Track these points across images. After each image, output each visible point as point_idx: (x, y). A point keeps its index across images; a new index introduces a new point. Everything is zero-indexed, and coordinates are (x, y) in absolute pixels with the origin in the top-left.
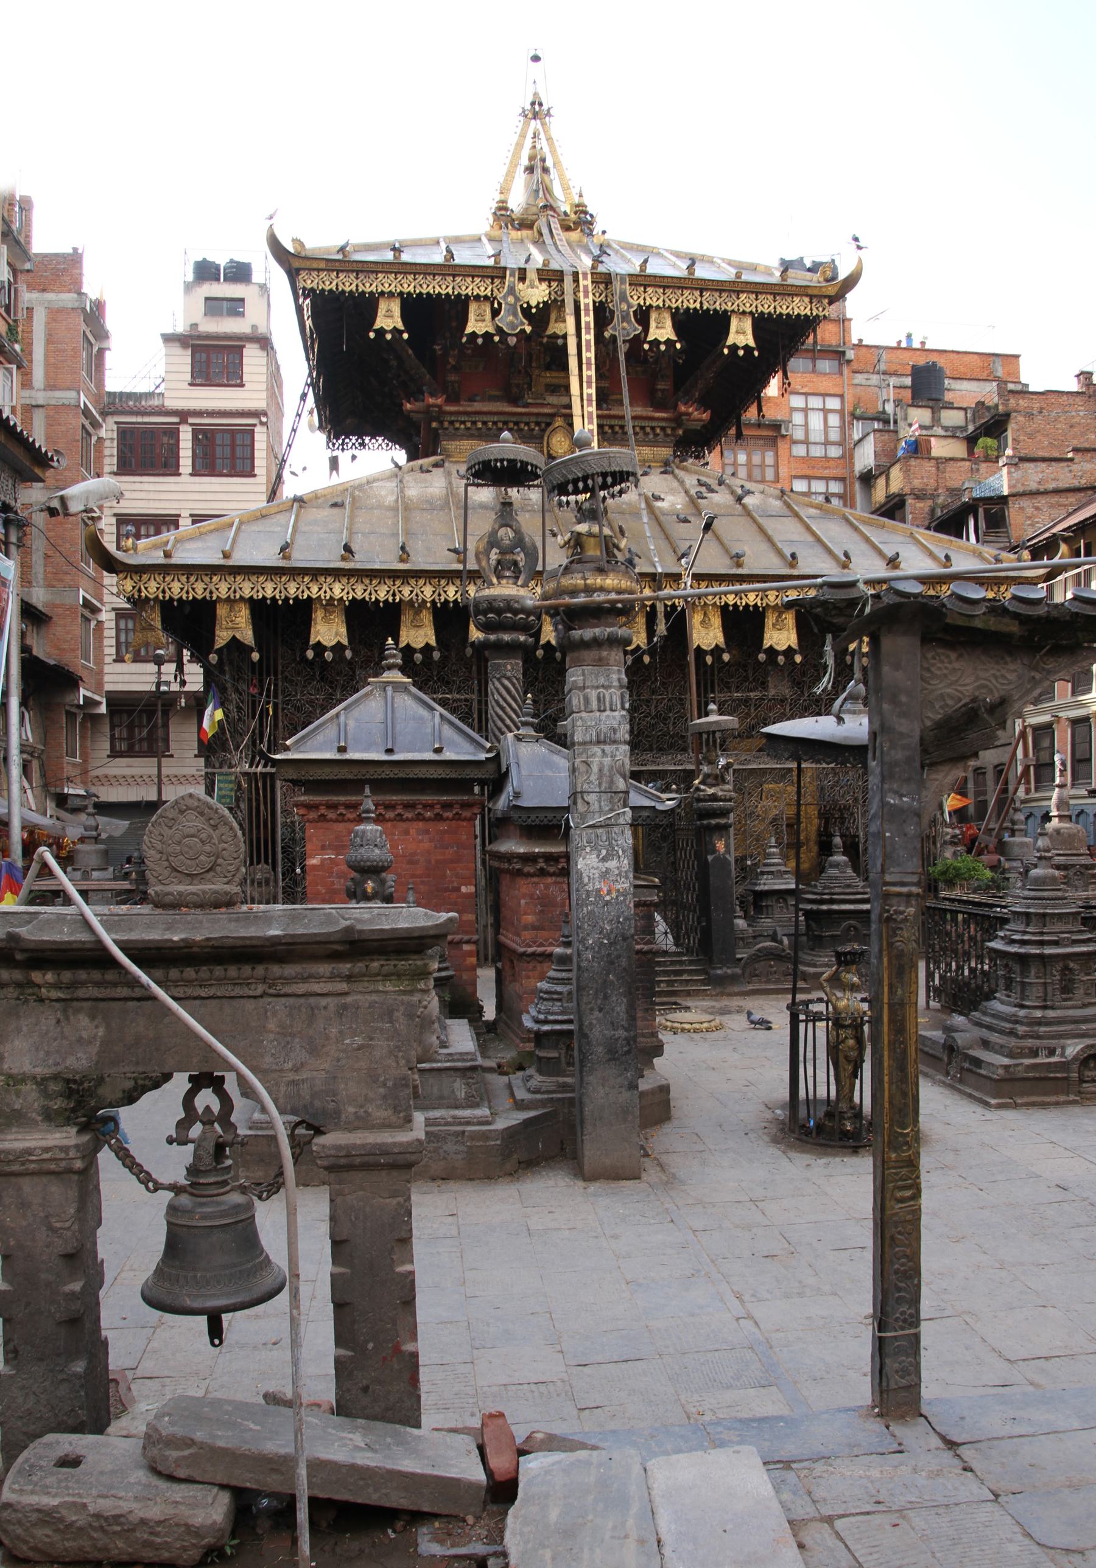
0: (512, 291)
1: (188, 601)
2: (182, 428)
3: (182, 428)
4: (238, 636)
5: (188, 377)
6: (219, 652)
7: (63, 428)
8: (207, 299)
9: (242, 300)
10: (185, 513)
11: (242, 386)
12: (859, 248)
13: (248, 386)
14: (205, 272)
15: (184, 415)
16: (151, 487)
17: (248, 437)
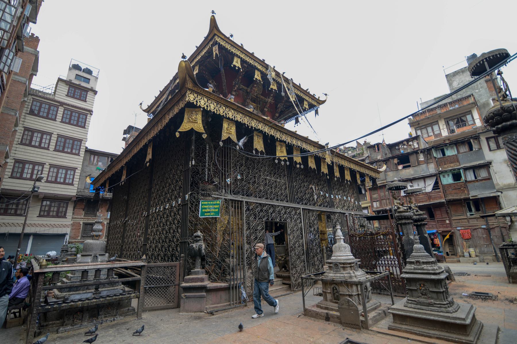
0: (270, 71)
1: (216, 114)
2: (60, 107)
3: (60, 107)
4: (230, 136)
5: (66, 93)
6: (223, 141)
7: (16, 89)
8: (77, 75)
9: (89, 79)
10: (56, 133)
11: (85, 101)
12: (326, 95)
13: (88, 102)
14: (76, 67)
15: (62, 104)
16: (43, 122)
17: (84, 117)
